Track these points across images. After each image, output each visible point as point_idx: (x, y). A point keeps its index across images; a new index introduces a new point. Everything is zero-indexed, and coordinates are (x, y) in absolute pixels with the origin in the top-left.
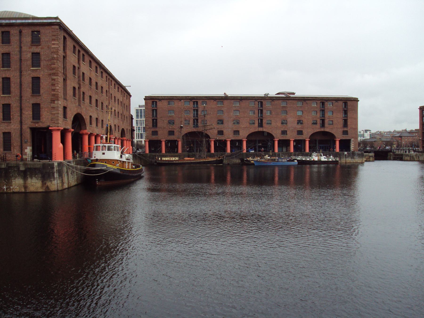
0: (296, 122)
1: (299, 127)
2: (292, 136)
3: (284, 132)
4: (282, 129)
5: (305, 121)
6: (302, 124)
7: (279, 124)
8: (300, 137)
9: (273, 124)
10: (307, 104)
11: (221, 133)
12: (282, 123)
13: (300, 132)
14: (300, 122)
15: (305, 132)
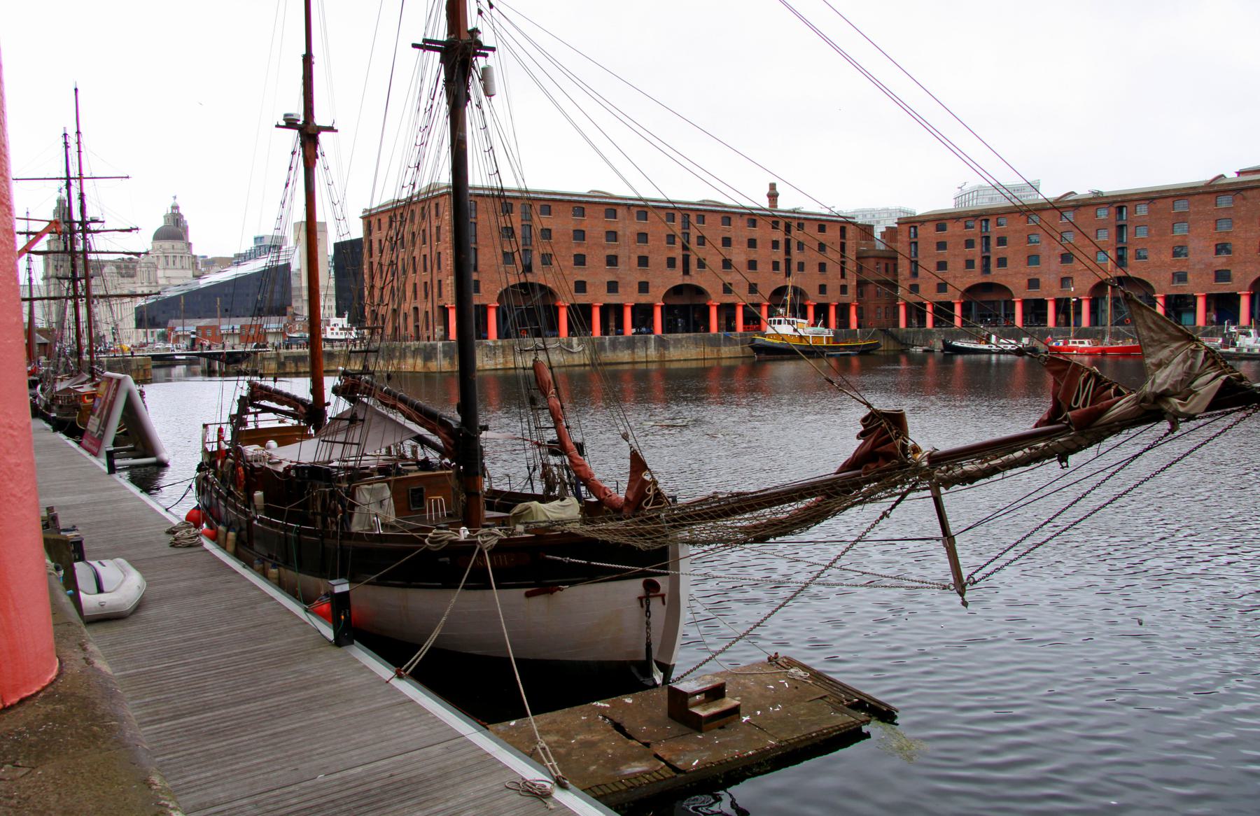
0: (1213, 249)
1: (1220, 261)
2: (1199, 286)
3: (1181, 277)
4: (1175, 270)
5: (1237, 244)
6: (1229, 252)
7: (1167, 257)
8: (1223, 288)
9: (1152, 258)
10: (1244, 199)
11: (1033, 283)
12: (1175, 254)
13: (1222, 275)
14: (1221, 248)
15: (1236, 273)
